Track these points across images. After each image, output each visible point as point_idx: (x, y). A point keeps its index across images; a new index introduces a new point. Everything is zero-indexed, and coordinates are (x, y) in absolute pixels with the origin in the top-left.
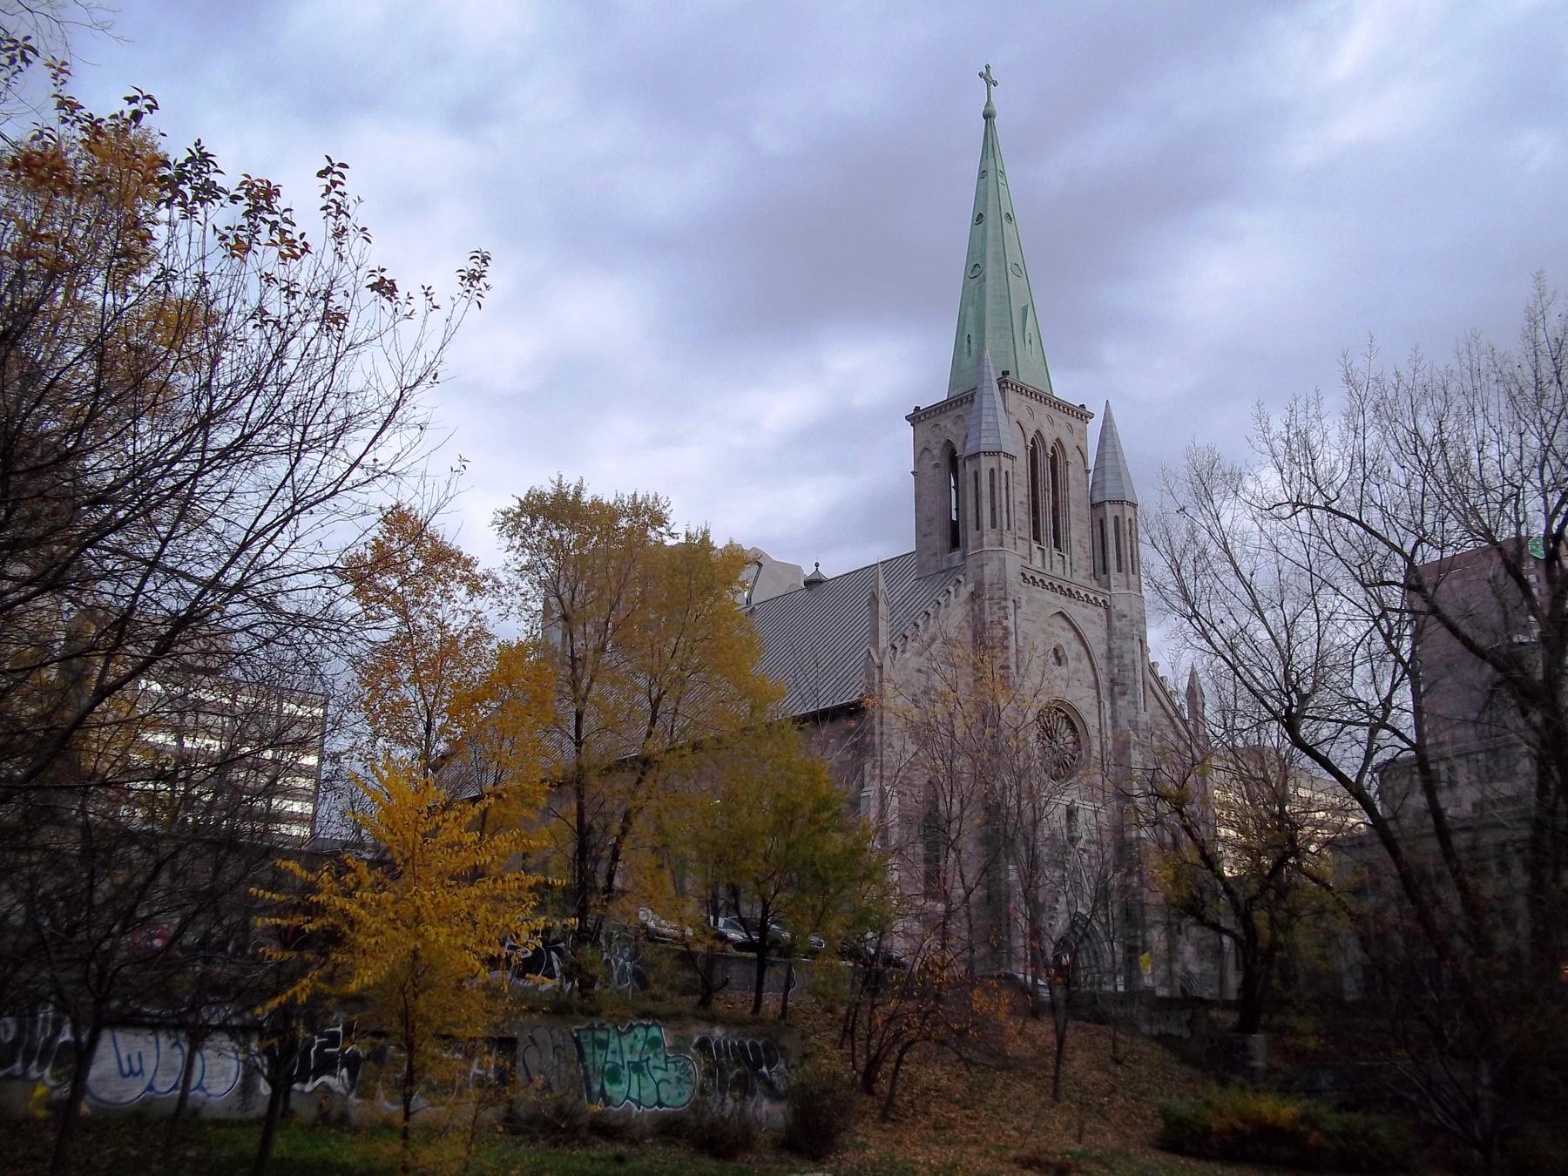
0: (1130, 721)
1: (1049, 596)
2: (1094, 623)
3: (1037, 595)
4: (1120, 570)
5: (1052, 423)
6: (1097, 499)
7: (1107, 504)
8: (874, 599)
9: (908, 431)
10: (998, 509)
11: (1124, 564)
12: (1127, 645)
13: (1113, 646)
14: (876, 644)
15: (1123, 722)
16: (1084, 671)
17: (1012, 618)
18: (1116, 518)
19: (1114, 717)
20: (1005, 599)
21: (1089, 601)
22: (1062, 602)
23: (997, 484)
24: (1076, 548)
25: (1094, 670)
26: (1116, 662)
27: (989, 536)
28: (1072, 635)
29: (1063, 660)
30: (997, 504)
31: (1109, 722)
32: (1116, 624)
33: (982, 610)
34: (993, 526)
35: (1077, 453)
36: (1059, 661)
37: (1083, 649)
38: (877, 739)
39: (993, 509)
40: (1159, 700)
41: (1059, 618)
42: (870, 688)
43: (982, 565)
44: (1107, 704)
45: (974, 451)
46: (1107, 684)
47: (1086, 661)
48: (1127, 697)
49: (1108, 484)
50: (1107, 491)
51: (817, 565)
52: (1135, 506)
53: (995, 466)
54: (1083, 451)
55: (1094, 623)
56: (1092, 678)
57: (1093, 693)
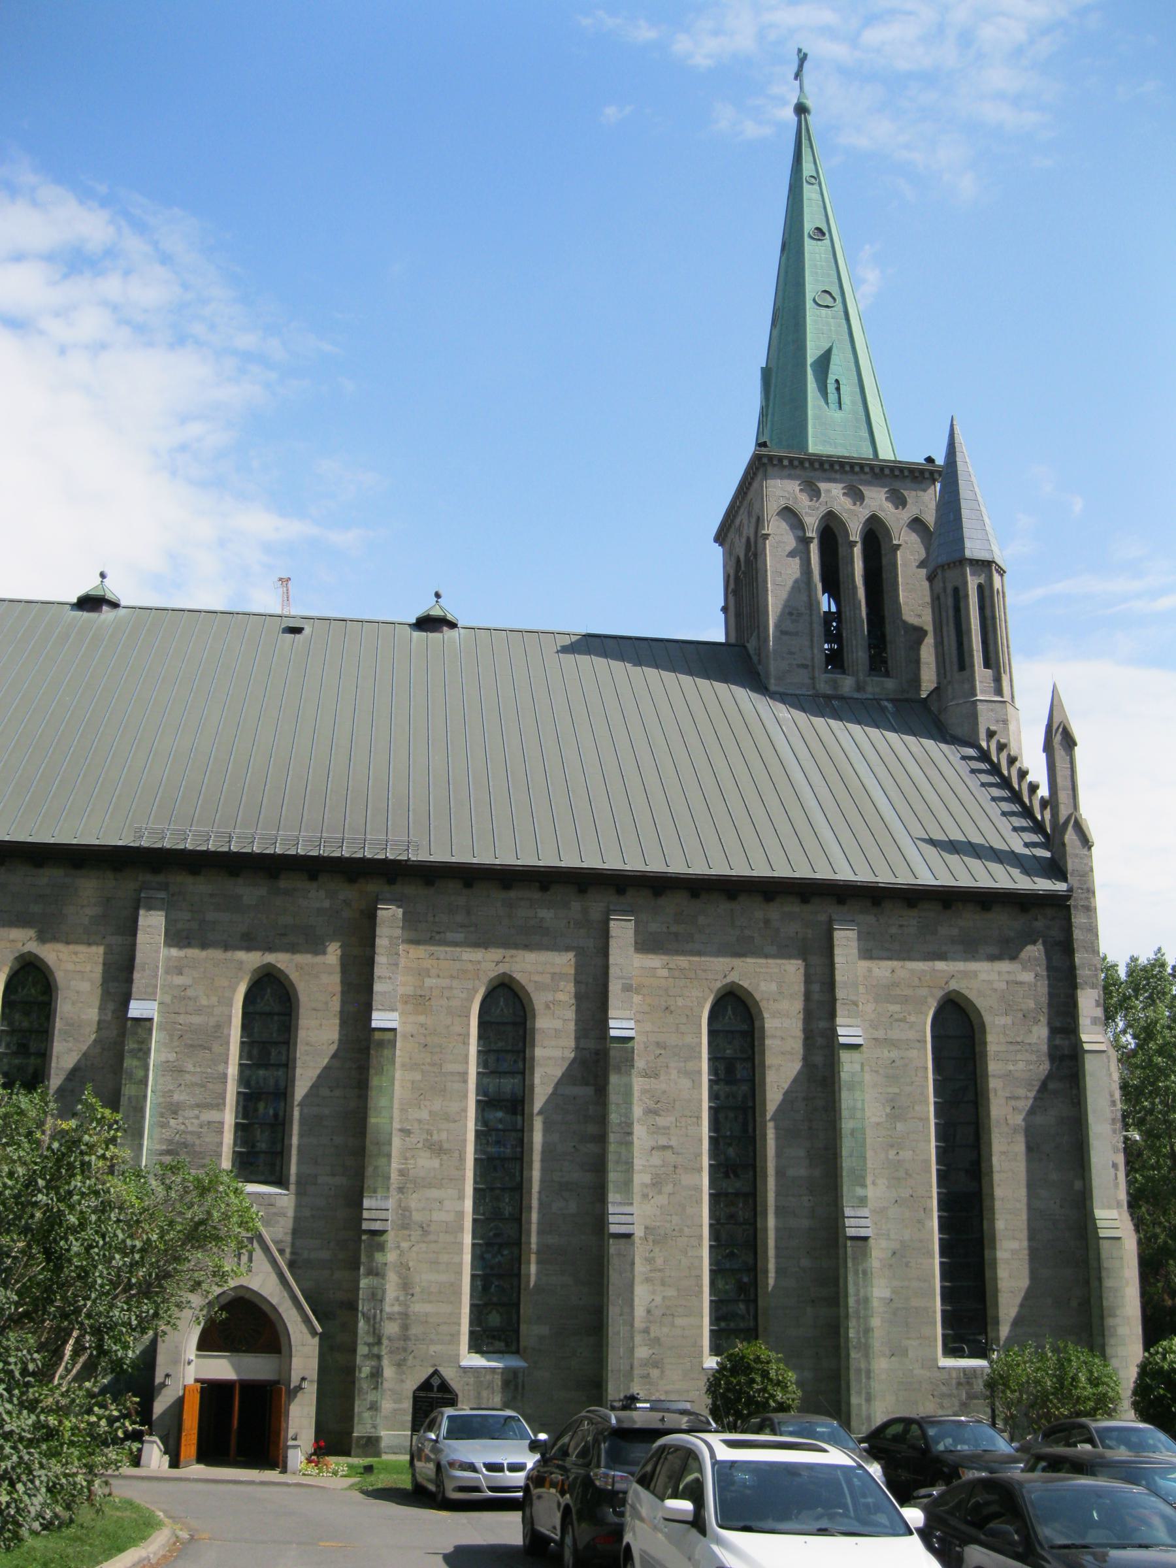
51: (438, 595)
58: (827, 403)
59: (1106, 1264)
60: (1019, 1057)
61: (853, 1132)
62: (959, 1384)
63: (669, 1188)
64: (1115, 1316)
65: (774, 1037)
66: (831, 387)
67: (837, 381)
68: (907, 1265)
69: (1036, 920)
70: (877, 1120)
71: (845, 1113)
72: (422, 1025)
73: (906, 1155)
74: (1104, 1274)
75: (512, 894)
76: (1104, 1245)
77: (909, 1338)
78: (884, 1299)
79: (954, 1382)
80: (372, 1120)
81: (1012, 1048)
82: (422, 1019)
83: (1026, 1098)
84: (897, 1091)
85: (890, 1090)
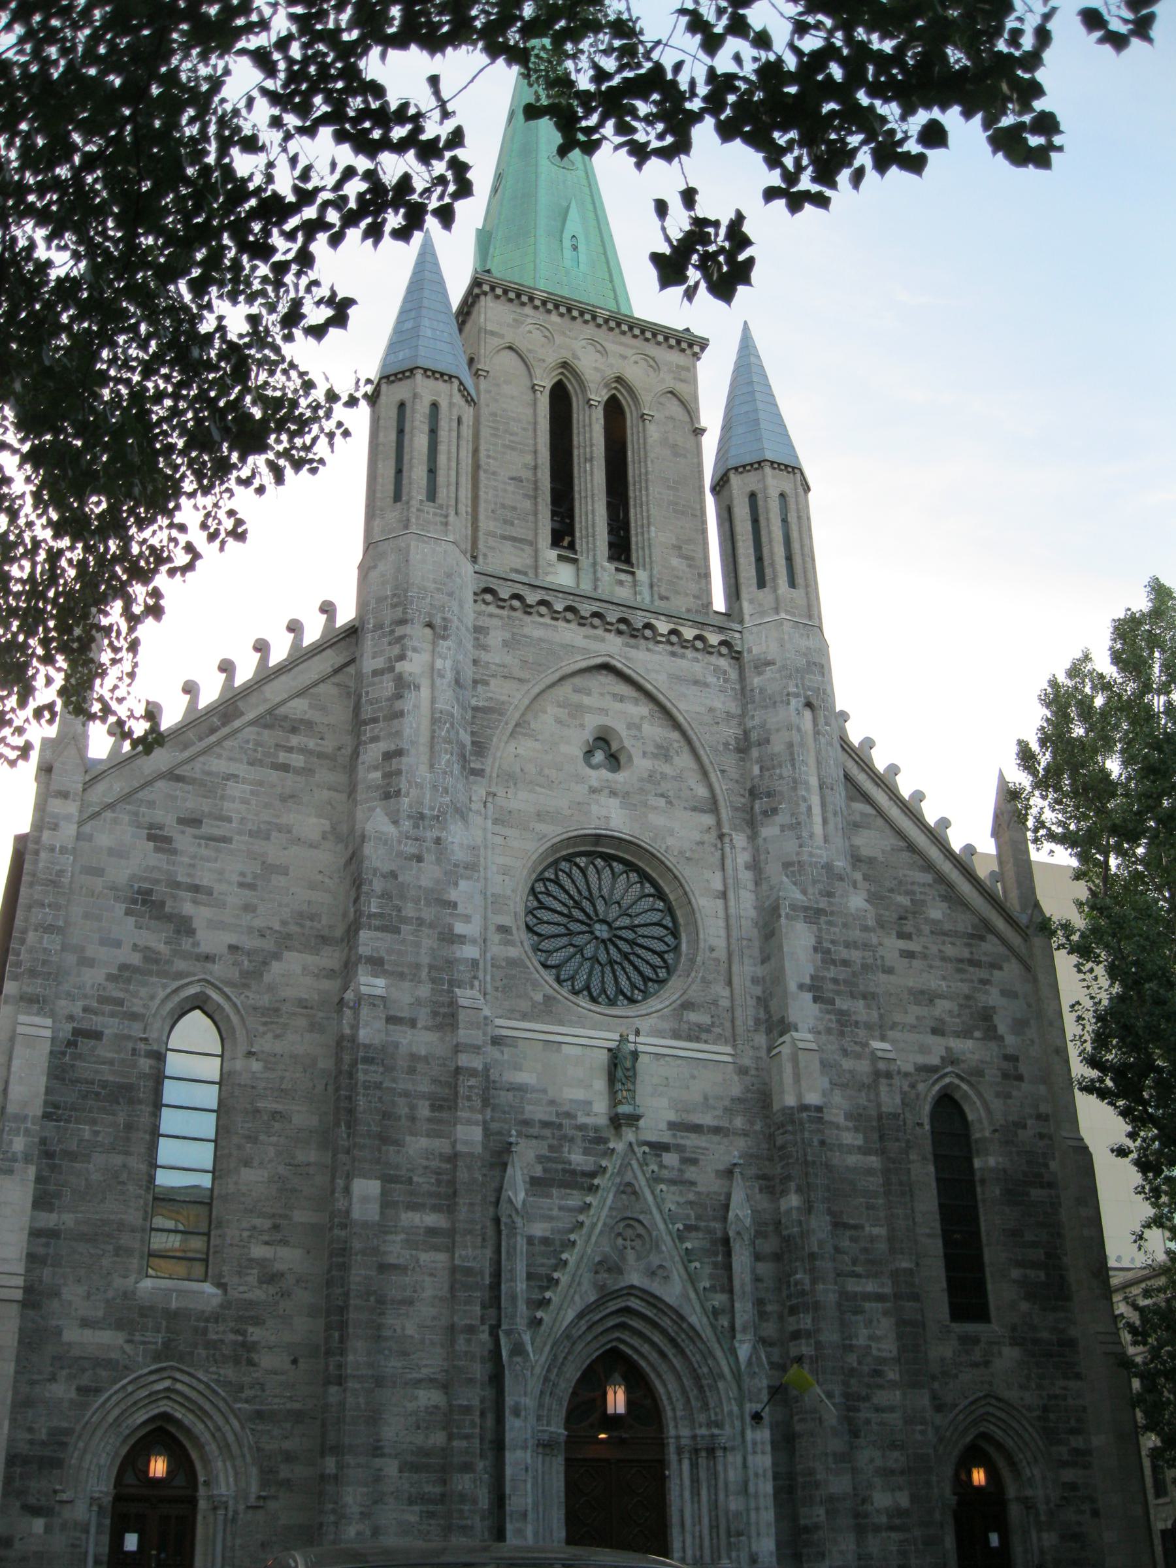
0: (787, 865)
1: (570, 633)
2: (706, 685)
3: (537, 633)
4: (761, 584)
5: (604, 352)
11: (768, 571)
12: (775, 718)
13: (750, 724)
15: (773, 869)
18: (753, 496)
19: (755, 866)
20: (403, 622)
22: (612, 647)
25: (705, 773)
26: (755, 753)
28: (643, 709)
29: (623, 760)
31: (746, 876)
32: (756, 681)
34: (397, 497)
35: (674, 408)
37: (676, 735)
40: (900, 834)
41: (607, 679)
44: (740, 840)
47: (684, 760)
48: (782, 818)
52: (793, 469)
54: (686, 397)
55: (696, 682)
56: (702, 791)
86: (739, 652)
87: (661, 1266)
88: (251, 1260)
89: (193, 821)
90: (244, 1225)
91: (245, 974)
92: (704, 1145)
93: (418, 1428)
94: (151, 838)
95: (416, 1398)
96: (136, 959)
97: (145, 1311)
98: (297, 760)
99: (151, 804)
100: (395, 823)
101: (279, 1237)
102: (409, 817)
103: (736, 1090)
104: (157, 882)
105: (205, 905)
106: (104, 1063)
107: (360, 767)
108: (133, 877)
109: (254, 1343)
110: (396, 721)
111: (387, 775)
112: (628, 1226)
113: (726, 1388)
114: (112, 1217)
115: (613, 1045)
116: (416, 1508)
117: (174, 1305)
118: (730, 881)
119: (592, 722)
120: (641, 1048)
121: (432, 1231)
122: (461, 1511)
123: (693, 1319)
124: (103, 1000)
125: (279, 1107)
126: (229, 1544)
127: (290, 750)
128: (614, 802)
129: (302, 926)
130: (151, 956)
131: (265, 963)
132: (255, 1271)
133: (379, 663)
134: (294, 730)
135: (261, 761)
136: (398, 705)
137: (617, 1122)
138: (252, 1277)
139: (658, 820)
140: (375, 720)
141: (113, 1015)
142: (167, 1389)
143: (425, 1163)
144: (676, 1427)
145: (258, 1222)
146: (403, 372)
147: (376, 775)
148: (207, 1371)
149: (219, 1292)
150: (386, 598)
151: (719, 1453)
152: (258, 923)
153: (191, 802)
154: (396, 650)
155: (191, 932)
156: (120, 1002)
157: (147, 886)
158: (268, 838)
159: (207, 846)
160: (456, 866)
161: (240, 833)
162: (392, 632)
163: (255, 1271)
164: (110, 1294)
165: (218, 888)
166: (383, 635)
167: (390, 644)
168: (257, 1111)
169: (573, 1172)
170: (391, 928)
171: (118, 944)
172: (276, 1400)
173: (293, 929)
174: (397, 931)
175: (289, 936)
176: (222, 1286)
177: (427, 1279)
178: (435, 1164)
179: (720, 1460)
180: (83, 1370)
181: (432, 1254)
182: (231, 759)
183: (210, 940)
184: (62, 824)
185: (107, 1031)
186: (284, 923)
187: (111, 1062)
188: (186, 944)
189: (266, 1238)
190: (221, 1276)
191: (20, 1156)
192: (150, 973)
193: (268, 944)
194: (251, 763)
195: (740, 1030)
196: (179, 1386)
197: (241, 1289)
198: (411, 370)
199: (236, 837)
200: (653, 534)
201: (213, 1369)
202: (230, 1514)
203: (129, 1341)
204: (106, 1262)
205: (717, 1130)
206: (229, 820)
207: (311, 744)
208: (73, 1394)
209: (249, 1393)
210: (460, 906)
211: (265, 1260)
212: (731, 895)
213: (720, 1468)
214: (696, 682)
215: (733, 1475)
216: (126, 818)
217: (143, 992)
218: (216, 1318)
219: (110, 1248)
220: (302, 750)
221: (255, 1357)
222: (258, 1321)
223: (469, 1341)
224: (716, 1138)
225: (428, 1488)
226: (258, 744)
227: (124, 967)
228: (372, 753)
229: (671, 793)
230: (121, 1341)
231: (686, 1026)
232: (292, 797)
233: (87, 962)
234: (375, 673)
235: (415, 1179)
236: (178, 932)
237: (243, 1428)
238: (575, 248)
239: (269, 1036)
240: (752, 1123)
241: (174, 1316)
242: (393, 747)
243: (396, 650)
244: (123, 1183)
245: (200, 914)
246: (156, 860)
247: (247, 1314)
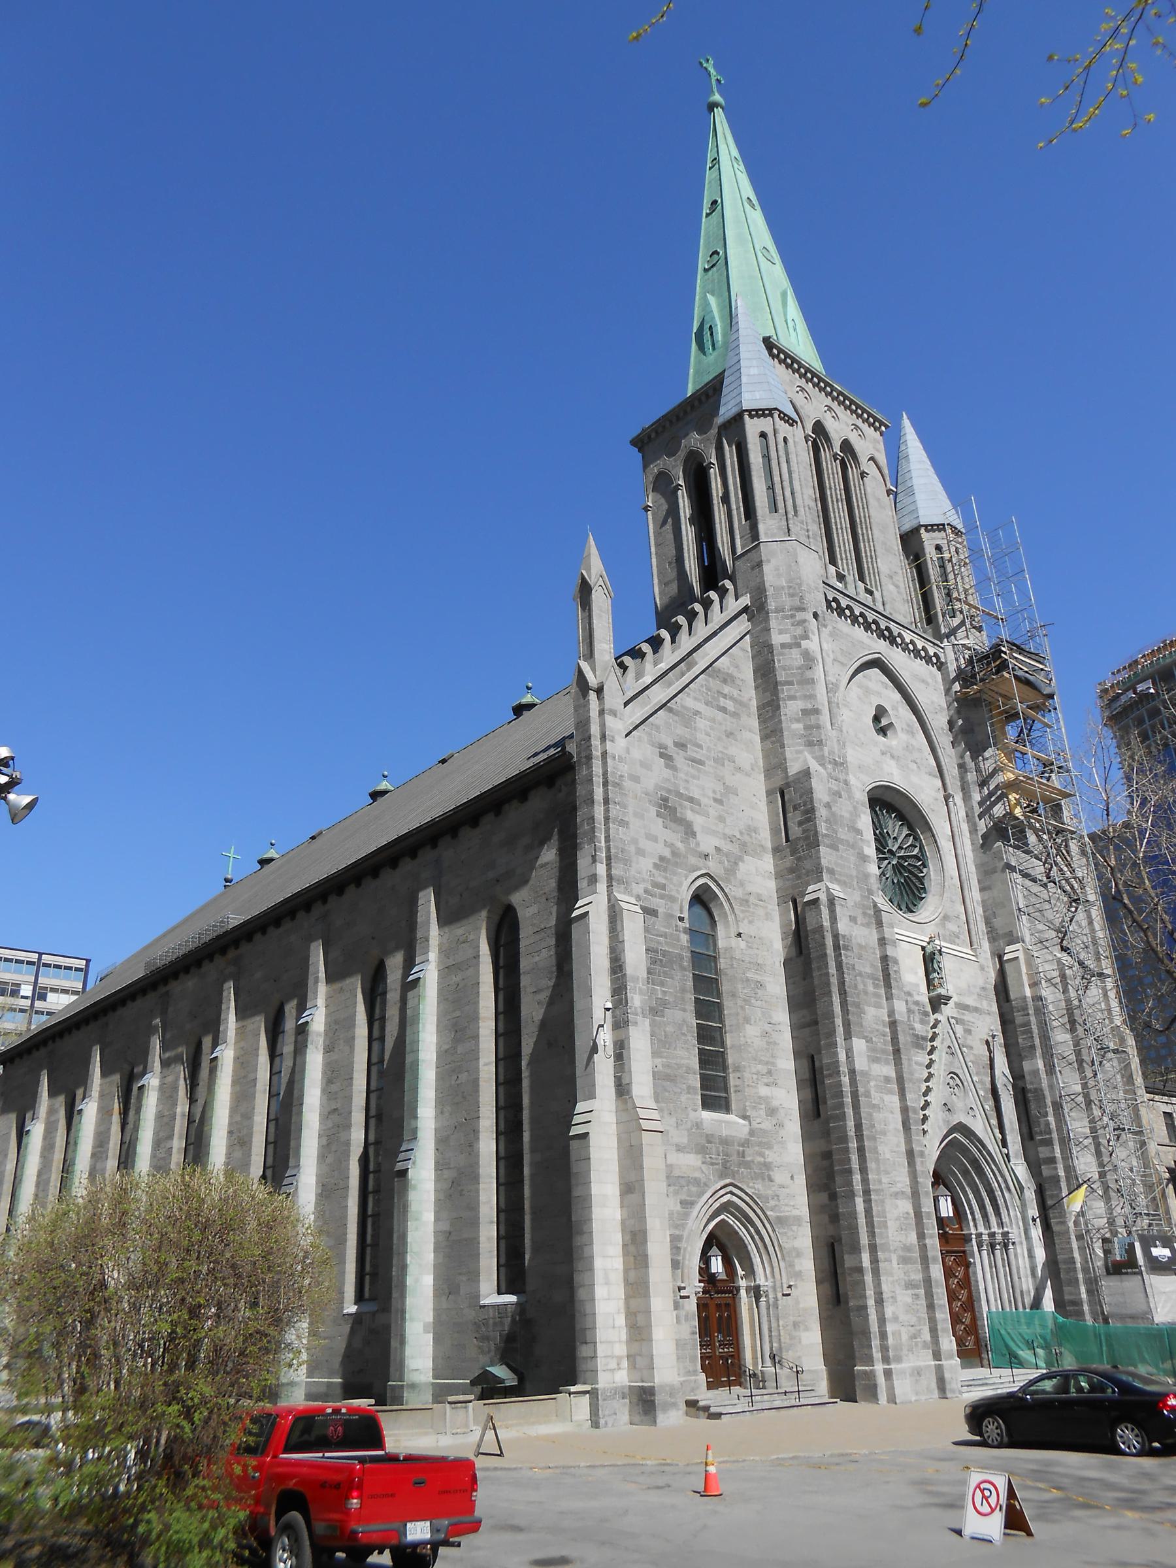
1: (859, 632)
2: (927, 684)
6: (907, 527)
7: (922, 531)
8: (585, 589)
9: (636, 456)
10: (778, 487)
14: (590, 655)
16: (920, 750)
17: (815, 638)
20: (802, 609)
21: (916, 653)
22: (881, 647)
23: (773, 454)
24: (889, 588)
27: (768, 525)
28: (897, 696)
30: (777, 479)
31: (965, 827)
33: (768, 630)
36: (883, 731)
38: (599, 812)
39: (771, 488)
42: (583, 724)
43: (759, 564)
44: (958, 798)
45: (734, 411)
46: (955, 771)
49: (920, 504)
50: (921, 512)
53: (769, 431)
55: (923, 681)
57: (939, 783)
58: (704, 354)
59: (574, 1169)
60: (544, 944)
61: (412, 1063)
62: (495, 1324)
63: (334, 1148)
64: (581, 1233)
65: (391, 990)
66: (707, 336)
67: (711, 327)
68: (461, 1194)
69: (560, 791)
70: (446, 1047)
71: (408, 1049)
72: (242, 1048)
73: (464, 1077)
74: (573, 1182)
75: (281, 929)
76: (574, 1144)
77: (460, 1274)
78: (445, 1232)
79: (491, 1321)
80: (206, 1129)
81: (538, 937)
82: (242, 1044)
83: (548, 988)
84: (458, 1013)
85: (455, 1015)
86: (942, 663)
87: (971, 1108)
88: (760, 1097)
89: (681, 745)
90: (754, 1070)
91: (728, 871)
92: (972, 1020)
93: (902, 1230)
94: (662, 755)
95: (897, 1206)
96: (667, 853)
97: (709, 1139)
98: (730, 705)
99: (657, 728)
100: (822, 765)
101: (771, 1079)
102: (830, 762)
103: (981, 983)
104: (669, 791)
105: (698, 813)
106: (661, 936)
107: (783, 718)
108: (658, 787)
109: (770, 1163)
110: (809, 686)
111: (807, 728)
112: (952, 1078)
113: (1012, 1199)
114: (682, 1061)
115: (925, 944)
116: (910, 1292)
117: (724, 1133)
118: (955, 829)
119: (877, 701)
120: (944, 950)
121: (887, 1079)
122: (937, 1293)
123: (990, 1148)
124: (656, 885)
125: (759, 978)
126: (774, 1325)
127: (725, 696)
128: (893, 763)
129: (751, 837)
130: (675, 853)
131: (736, 864)
132: (763, 1107)
133: (786, 638)
134: (725, 681)
135: (711, 702)
136: (808, 674)
137: (937, 1003)
138: (763, 1113)
139: (915, 779)
140: (790, 683)
141: (662, 897)
142: (729, 1202)
143: (877, 1027)
144: (976, 1226)
145: (760, 1067)
146: (763, 410)
147: (798, 727)
148: (748, 1186)
149: (746, 1123)
150: (783, 588)
151: (1011, 1246)
152: (728, 832)
153: (681, 731)
154: (799, 631)
155: (694, 834)
156: (663, 887)
157: (665, 794)
158: (723, 765)
159: (693, 766)
160: (857, 803)
161: (708, 758)
162: (792, 616)
163: (763, 1107)
164: (689, 1125)
165: (704, 801)
166: (786, 617)
167: (793, 625)
168: (748, 980)
169: (917, 1036)
170: (834, 847)
171: (655, 839)
172: (787, 1208)
173: (746, 838)
174: (837, 850)
175: (744, 845)
176: (745, 1117)
177: (891, 1115)
178: (881, 1028)
179: (1011, 1252)
180: (682, 1187)
181: (890, 1096)
182: (695, 699)
183: (707, 843)
184: (616, 737)
185: (660, 910)
186: (741, 833)
187: (665, 935)
188: (692, 842)
189: (766, 1081)
190: (745, 1109)
191: (639, 1010)
192: (676, 864)
193: (734, 849)
194: (707, 704)
195: (974, 938)
196: (735, 1199)
197: (758, 1120)
198: (770, 410)
199: (707, 762)
200: (879, 565)
201: (751, 1185)
202: (771, 1301)
203: (703, 1163)
204: (684, 1098)
205: (976, 1010)
206: (700, 747)
207: (735, 693)
208: (678, 1207)
209: (772, 1203)
210: (864, 834)
211: (767, 1097)
212: (957, 838)
213: (1012, 1257)
214: (923, 681)
215: (1023, 1263)
216: (645, 738)
217: (675, 878)
218: (746, 1143)
219: (684, 1086)
220: (732, 698)
221: (771, 1173)
222: (770, 1147)
223: (922, 1162)
224: (976, 1015)
225: (913, 1277)
226: (709, 689)
227: (662, 859)
228: (791, 708)
229: (918, 761)
230: (699, 1163)
231: (948, 933)
232: (731, 734)
233: (641, 852)
234: (783, 646)
235: (874, 1039)
236: (686, 834)
237: (774, 1231)
238: (795, 330)
239: (746, 921)
240: (991, 1006)
241: (725, 1142)
242: (810, 706)
243: (799, 631)
244: (684, 1034)
245: (698, 821)
246: (667, 773)
247: (765, 1140)
